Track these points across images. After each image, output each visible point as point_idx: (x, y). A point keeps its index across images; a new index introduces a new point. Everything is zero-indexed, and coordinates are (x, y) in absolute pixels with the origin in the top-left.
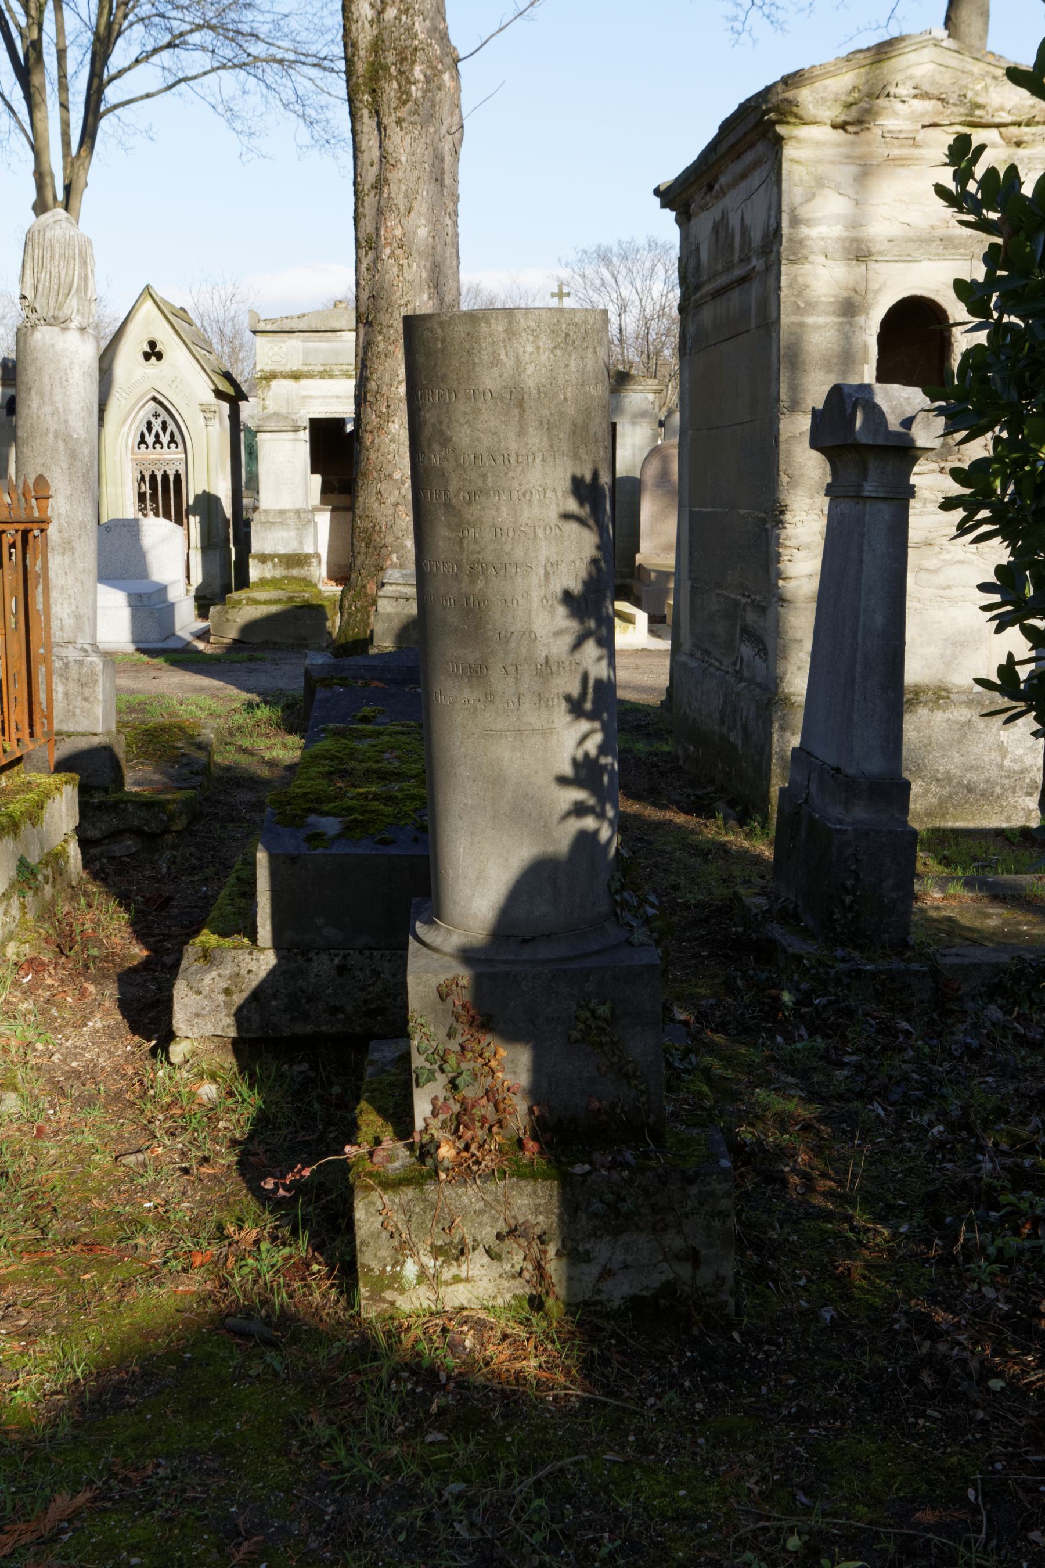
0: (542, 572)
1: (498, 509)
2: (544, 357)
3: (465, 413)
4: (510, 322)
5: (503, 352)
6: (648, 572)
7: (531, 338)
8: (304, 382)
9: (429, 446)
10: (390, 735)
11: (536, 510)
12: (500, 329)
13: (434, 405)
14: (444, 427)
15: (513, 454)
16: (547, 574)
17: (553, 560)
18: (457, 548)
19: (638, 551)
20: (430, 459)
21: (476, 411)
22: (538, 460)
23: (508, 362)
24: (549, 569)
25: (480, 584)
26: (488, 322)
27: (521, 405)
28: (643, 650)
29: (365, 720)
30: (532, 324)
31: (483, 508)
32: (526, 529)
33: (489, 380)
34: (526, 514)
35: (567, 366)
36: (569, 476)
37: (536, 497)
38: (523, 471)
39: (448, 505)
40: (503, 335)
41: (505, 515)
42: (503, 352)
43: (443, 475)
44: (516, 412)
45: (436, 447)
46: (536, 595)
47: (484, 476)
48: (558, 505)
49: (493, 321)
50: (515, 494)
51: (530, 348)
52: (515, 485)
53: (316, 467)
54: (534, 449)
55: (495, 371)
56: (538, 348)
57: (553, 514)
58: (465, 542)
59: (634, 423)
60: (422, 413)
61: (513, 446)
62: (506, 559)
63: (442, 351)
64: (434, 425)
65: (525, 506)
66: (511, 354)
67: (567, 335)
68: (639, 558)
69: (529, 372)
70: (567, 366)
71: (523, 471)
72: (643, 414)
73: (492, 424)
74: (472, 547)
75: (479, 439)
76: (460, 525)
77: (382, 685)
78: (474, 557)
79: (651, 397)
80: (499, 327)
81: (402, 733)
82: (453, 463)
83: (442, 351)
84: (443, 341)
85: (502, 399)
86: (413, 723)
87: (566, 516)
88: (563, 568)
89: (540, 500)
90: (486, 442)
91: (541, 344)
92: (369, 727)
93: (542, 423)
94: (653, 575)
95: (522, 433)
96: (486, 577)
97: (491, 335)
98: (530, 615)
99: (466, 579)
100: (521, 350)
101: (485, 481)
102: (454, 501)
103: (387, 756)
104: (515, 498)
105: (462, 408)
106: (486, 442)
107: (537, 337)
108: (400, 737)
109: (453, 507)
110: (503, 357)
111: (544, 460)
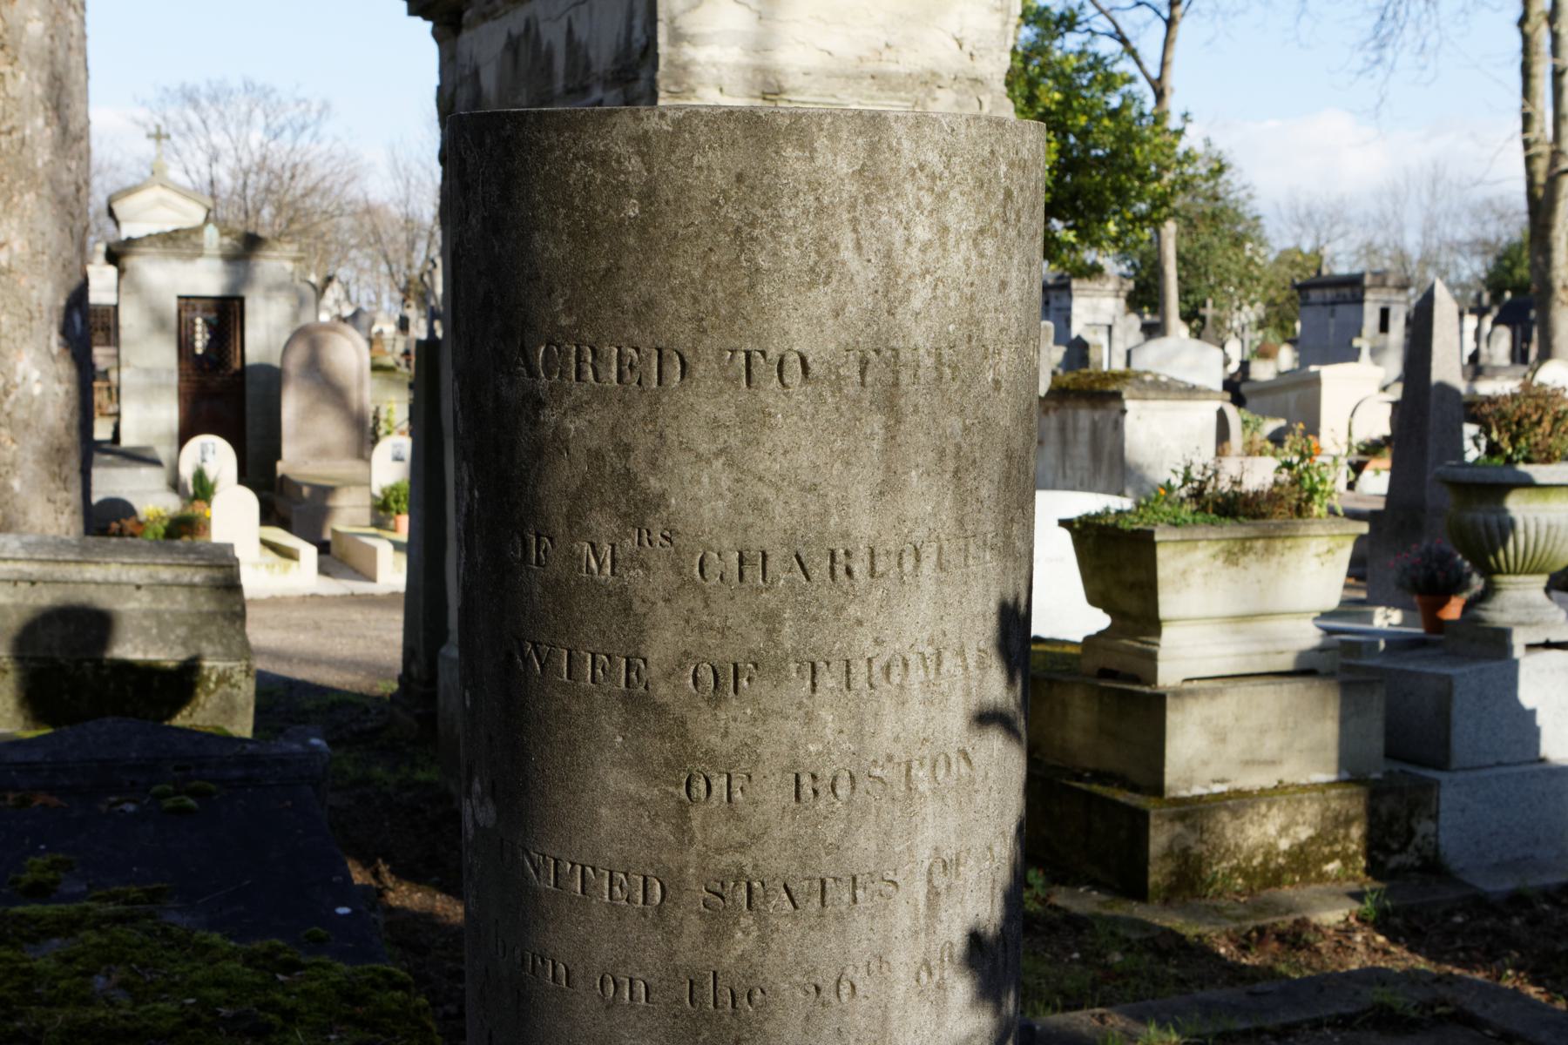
0: (920, 890)
1: (809, 718)
2: (956, 260)
3: (716, 424)
4: (873, 149)
5: (847, 239)
6: (298, 486)
7: (927, 200)
8: (1541, 640)
9: (575, 518)
10: (96, 927)
11: (916, 713)
12: (843, 167)
13: (601, 395)
14: (638, 462)
15: (862, 552)
16: (933, 894)
17: (948, 854)
18: (664, 830)
19: (277, 455)
20: (573, 557)
21: (756, 420)
22: (928, 566)
23: (860, 269)
24: (940, 882)
25: (742, 941)
26: (806, 145)
27: (890, 404)
28: (312, 596)
29: (39, 892)
30: (933, 158)
31: (764, 715)
32: (889, 773)
33: (804, 323)
34: (889, 727)
35: (1003, 285)
36: (993, 606)
37: (916, 675)
38: (887, 598)
39: (638, 702)
40: (851, 188)
41: (829, 734)
42: (847, 239)
43: (627, 608)
44: (876, 423)
45: (602, 524)
46: (903, 960)
47: (771, 620)
48: (968, 693)
49: (821, 142)
50: (860, 671)
51: (922, 233)
52: (864, 642)
54: (920, 533)
55: (822, 298)
56: (945, 229)
57: (955, 720)
58: (696, 816)
59: (268, 298)
60: (550, 416)
61: (864, 526)
62: (827, 866)
63: (642, 227)
64: (596, 456)
65: (888, 703)
66: (871, 247)
67: (1008, 195)
68: (281, 468)
69: (916, 303)
70: (1003, 285)
71: (887, 598)
72: (280, 287)
73: (803, 459)
74: (720, 831)
75: (759, 506)
76: (685, 770)
77: (54, 801)
78: (727, 860)
79: (289, 266)
80: (838, 162)
81: (119, 919)
82: (663, 577)
83: (642, 227)
84: (648, 195)
85: (838, 385)
86: (134, 891)
87: (985, 718)
88: (970, 871)
89: (927, 684)
90: (783, 513)
91: (950, 219)
92: (50, 910)
93: (942, 454)
94: (306, 491)
95: (888, 488)
96: (762, 920)
97: (814, 186)
98: (885, 1019)
99: (694, 926)
100: (898, 236)
101: (771, 632)
102: (662, 691)
103: (99, 982)
104: (860, 681)
105: (707, 408)
106: (783, 513)
107: (942, 196)
108: (118, 930)
109: (660, 710)
110: (847, 254)
111: (940, 566)
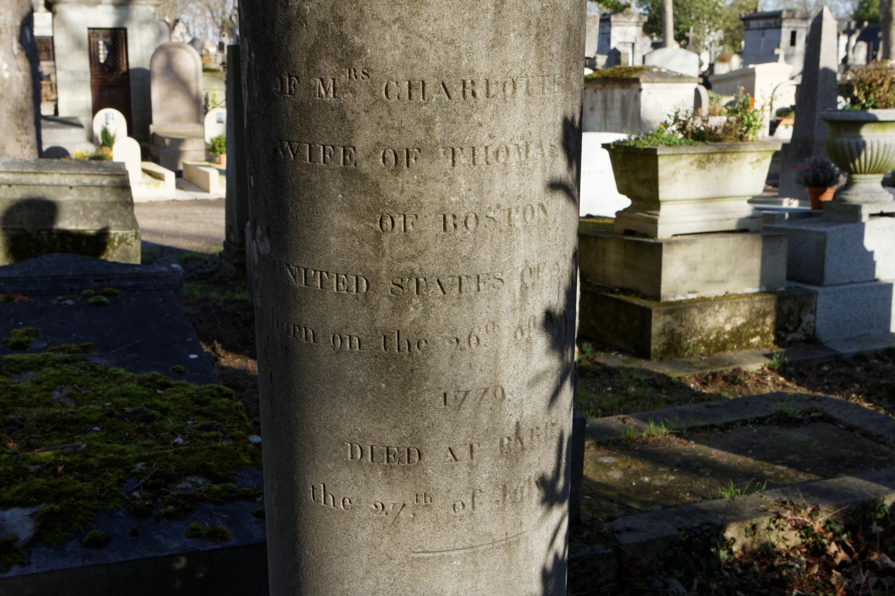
0: (517, 284)
1: (451, 182)
6: (162, 139)
9: (311, 64)
10: (53, 365)
11: (514, 180)
14: (348, 28)
15: (481, 82)
16: (524, 287)
17: (533, 265)
18: (368, 249)
19: (150, 121)
20: (311, 88)
22: (521, 92)
24: (528, 280)
25: (414, 313)
28: (173, 200)
29: (19, 347)
31: (425, 179)
32: (499, 215)
34: (498, 188)
36: (559, 120)
37: (514, 157)
38: (496, 111)
39: (351, 173)
43: (343, 117)
45: (328, 67)
46: (507, 325)
47: (428, 122)
48: (545, 171)
50: (480, 153)
52: (483, 137)
53: (618, 213)
54: (516, 72)
57: (537, 186)
58: (386, 240)
59: (140, 29)
61: (483, 66)
62: (462, 269)
64: (323, 25)
65: (498, 174)
68: (153, 128)
71: (496, 111)
72: (147, 22)
73: (446, 24)
74: (400, 248)
75: (420, 53)
76: (380, 213)
77: (27, 299)
78: (404, 265)
79: (152, 9)
81: (66, 361)
86: (74, 346)
88: (546, 276)
89: (520, 164)
90: (434, 58)
92: (26, 357)
93: (529, 23)
94: (167, 142)
95: (497, 43)
96: (425, 300)
98: (497, 358)
99: (386, 304)
101: (428, 130)
102: (365, 166)
103: (56, 394)
104: (481, 160)
106: (434, 58)
108: (65, 367)
109: (364, 177)
111: (528, 92)
